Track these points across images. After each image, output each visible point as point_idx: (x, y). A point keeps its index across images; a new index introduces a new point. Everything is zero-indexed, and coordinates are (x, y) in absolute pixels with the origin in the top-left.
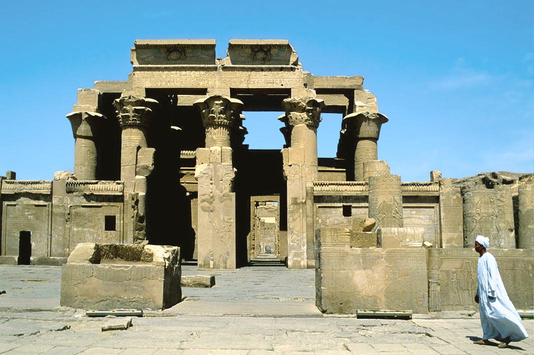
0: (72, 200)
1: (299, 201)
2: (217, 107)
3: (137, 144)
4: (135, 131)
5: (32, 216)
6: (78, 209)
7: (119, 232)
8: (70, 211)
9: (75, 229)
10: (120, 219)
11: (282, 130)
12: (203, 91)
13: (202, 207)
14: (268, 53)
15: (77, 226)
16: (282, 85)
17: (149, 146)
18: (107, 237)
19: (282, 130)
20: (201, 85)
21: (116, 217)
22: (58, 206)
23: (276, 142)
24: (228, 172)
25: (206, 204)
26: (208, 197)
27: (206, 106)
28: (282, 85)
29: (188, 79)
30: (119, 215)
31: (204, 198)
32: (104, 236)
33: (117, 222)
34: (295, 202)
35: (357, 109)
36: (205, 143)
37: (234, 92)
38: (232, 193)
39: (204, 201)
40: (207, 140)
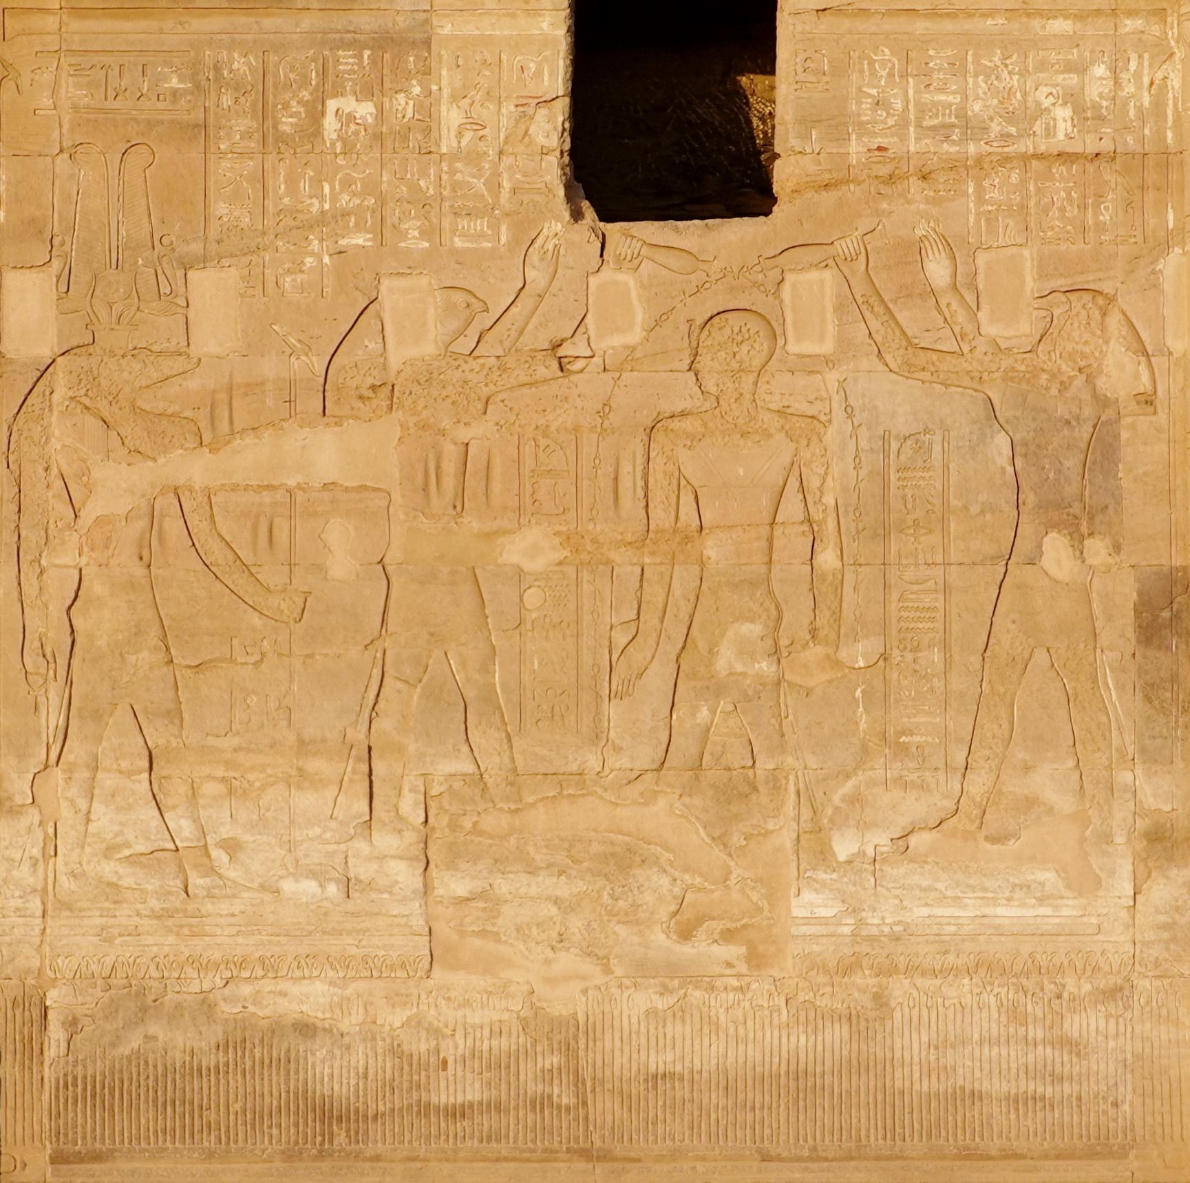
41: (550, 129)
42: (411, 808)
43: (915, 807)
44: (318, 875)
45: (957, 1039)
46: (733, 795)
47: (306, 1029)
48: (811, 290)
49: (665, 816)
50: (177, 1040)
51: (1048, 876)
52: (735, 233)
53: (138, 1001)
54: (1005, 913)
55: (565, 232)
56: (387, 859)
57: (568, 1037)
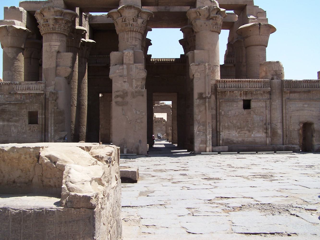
1: (204, 96)
3: (57, 48)
4: (55, 37)
6: (4, 106)
7: (41, 126)
11: (181, 42)
17: (67, 51)
18: (30, 129)
19: (181, 42)
21: (39, 112)
23: (176, 52)
24: (140, 72)
25: (119, 99)
26: (122, 93)
30: (41, 111)
31: (118, 94)
32: (28, 128)
33: (39, 116)
34: (201, 96)
35: (250, 21)
36: (118, 48)
39: (117, 96)
41: (242, 106)
42: (238, 132)
43: (257, 132)
44: (234, 134)
45: (258, 140)
46: (249, 131)
47: (234, 140)
48: (252, 112)
49: (247, 132)
50: (229, 140)
51: (261, 134)
52: (249, 110)
53: (227, 139)
54: (259, 135)
55: (243, 110)
56: (236, 133)
57: (244, 140)
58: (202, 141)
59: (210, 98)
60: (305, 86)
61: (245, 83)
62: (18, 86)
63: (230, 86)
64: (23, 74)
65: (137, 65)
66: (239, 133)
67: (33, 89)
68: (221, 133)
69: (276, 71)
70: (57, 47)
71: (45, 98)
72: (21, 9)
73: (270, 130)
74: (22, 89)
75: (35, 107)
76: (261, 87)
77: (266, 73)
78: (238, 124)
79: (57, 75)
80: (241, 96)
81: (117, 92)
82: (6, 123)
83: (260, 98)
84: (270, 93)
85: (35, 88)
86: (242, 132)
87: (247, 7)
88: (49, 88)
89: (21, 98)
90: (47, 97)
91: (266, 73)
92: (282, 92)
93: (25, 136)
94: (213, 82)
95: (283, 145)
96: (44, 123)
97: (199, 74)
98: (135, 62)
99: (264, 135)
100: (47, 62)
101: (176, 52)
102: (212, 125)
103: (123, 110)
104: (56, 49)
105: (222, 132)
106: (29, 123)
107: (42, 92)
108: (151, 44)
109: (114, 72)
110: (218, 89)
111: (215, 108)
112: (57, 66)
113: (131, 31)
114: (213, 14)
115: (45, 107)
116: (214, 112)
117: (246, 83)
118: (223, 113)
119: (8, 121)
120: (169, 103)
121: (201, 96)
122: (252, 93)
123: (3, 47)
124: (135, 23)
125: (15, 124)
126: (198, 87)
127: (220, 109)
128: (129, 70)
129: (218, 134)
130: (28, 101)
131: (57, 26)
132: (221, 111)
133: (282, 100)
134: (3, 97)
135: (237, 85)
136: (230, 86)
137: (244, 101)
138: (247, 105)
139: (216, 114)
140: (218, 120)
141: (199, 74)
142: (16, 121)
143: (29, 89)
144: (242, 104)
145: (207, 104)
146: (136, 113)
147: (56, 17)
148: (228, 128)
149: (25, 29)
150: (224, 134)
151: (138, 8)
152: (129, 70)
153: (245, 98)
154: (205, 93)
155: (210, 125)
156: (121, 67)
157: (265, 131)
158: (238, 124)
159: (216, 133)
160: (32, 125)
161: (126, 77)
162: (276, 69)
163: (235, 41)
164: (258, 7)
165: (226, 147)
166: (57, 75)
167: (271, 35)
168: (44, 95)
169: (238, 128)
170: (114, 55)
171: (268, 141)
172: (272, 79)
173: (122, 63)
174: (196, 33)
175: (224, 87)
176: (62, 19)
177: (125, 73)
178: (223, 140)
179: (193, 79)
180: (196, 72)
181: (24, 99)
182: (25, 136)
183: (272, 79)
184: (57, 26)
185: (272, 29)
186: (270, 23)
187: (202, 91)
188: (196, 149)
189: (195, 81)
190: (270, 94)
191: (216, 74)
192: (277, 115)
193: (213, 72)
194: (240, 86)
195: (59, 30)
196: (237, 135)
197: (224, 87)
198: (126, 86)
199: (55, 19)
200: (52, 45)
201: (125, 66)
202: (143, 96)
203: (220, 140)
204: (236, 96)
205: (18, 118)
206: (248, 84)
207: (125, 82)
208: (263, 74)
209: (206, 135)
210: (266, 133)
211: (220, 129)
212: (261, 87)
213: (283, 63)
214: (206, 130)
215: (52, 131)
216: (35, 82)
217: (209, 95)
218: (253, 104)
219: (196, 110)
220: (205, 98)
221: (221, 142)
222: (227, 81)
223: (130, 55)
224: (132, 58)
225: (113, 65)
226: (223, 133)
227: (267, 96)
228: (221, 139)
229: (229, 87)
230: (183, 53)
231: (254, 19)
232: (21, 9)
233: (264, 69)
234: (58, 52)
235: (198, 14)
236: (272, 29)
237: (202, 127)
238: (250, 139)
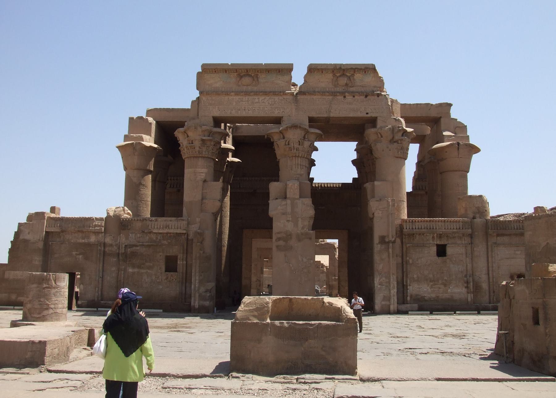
0: (127, 238)
1: (387, 240)
2: (294, 136)
3: (203, 176)
4: (201, 162)
5: (81, 256)
6: (134, 248)
8: (125, 250)
9: (130, 270)
10: (183, 260)
11: (354, 162)
12: (277, 121)
13: (277, 247)
14: (351, 78)
15: (134, 266)
16: (367, 114)
18: (167, 278)
20: (276, 113)
21: (179, 257)
22: (111, 245)
23: (347, 174)
24: (306, 209)
25: (281, 243)
26: (285, 235)
27: (282, 137)
28: (367, 114)
29: (262, 107)
30: (181, 255)
31: (279, 236)
33: (178, 262)
36: (278, 176)
37: (312, 120)
38: (312, 232)
39: (279, 239)
40: (281, 173)
41: (436, 252)
46: (445, 285)
48: (448, 261)
49: (442, 286)
52: (445, 258)
53: (417, 295)
58: (384, 297)
59: (394, 242)
60: (516, 228)
61: (439, 223)
62: (153, 223)
63: (420, 227)
64: (150, 203)
65: (304, 200)
66: (431, 287)
67: (173, 227)
68: (409, 287)
69: (478, 208)
70: (204, 175)
71: (187, 239)
72: (150, 119)
73: (472, 284)
74: (159, 227)
75: (174, 251)
76: (460, 229)
77: (466, 210)
78: (431, 276)
79: (202, 211)
80: (433, 241)
81: (278, 233)
82: (136, 270)
83: (459, 242)
84: (471, 236)
85: (170, 225)
86: (436, 286)
87: (442, 119)
88: (193, 226)
89: (157, 238)
90: (190, 238)
91: (466, 210)
92: (487, 235)
93: (161, 287)
94: (398, 222)
95: (490, 303)
96: (185, 271)
97: (380, 212)
98: (301, 197)
99: (464, 290)
100: (190, 193)
101: (347, 174)
102: (397, 277)
103: (285, 256)
104: (202, 177)
105: (410, 285)
106: (166, 271)
107: (185, 232)
108: (315, 165)
109: (275, 208)
110: (405, 230)
111: (401, 255)
112: (202, 199)
113: (295, 156)
114: (398, 136)
115: (187, 251)
116: (400, 260)
117: (440, 224)
118: (411, 261)
119: (139, 267)
120: (336, 241)
121: (383, 240)
122: (447, 236)
123: (126, 169)
124: (300, 147)
125: (149, 271)
126: (380, 228)
127: (407, 256)
128: (293, 206)
129: (405, 288)
130: (165, 242)
131: (204, 149)
132: (408, 258)
133: (487, 245)
134: (134, 237)
135: (429, 226)
136: (420, 227)
137: (438, 246)
138: (441, 251)
139: (403, 262)
140: (404, 270)
141: (380, 212)
142: (149, 268)
143: (167, 227)
144: (436, 250)
145: (390, 250)
146: (302, 260)
147: (204, 138)
148: (418, 281)
149: (156, 146)
150: (413, 289)
151: (305, 129)
152: (293, 206)
153: (438, 243)
154: (388, 236)
155: (395, 277)
156: (284, 203)
157: (466, 285)
158: (431, 276)
159: (402, 287)
160: (170, 274)
161: (289, 213)
162: (480, 204)
163: (426, 161)
164: (456, 119)
165: (416, 306)
166: (202, 211)
167: (474, 156)
168: (186, 236)
169: (430, 281)
170: (274, 187)
171: (470, 297)
172: (474, 218)
173: (286, 198)
174: (376, 158)
175: (412, 229)
176: (210, 140)
177: (289, 210)
178: (411, 296)
179: (373, 218)
180: (376, 210)
181: (160, 240)
182: (161, 287)
183: (474, 218)
184: (204, 149)
185: (476, 150)
186: (472, 141)
187: (384, 234)
188: (377, 307)
189: (375, 220)
190: (472, 238)
191: (402, 212)
192: (481, 264)
193: (399, 209)
194: (432, 227)
195: (207, 153)
196: (430, 290)
197: (412, 229)
198: (290, 227)
199: (203, 140)
200: (196, 174)
201: (289, 202)
202: (310, 239)
203: (407, 296)
204: (428, 240)
205: (151, 264)
206: (443, 224)
207: (288, 221)
208: (462, 211)
209: (390, 290)
210: (467, 287)
211: (407, 282)
212: (460, 229)
213: (488, 198)
214: (389, 282)
215: (197, 281)
216: (175, 218)
217: (393, 239)
218: (449, 251)
219: (376, 258)
220: (388, 242)
221: (409, 298)
222: (415, 221)
223: (295, 187)
224: (297, 192)
225: (274, 199)
226: (411, 287)
227: (467, 240)
228: (409, 295)
229: (418, 229)
230: (356, 176)
231: (451, 136)
232: (150, 119)
233: (464, 205)
234: (205, 181)
235: (379, 136)
236: (476, 150)
237: (384, 279)
238: (446, 296)
